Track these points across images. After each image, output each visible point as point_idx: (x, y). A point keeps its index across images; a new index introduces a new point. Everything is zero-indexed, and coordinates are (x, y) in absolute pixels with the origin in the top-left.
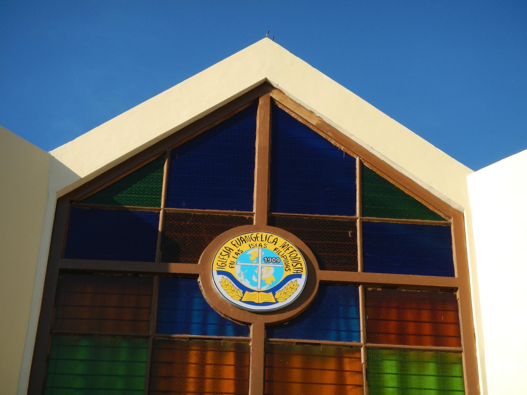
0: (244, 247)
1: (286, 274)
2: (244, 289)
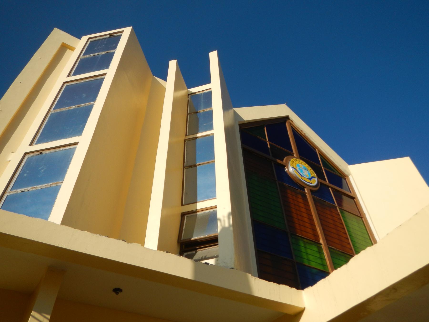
0: (297, 162)
2: (302, 176)
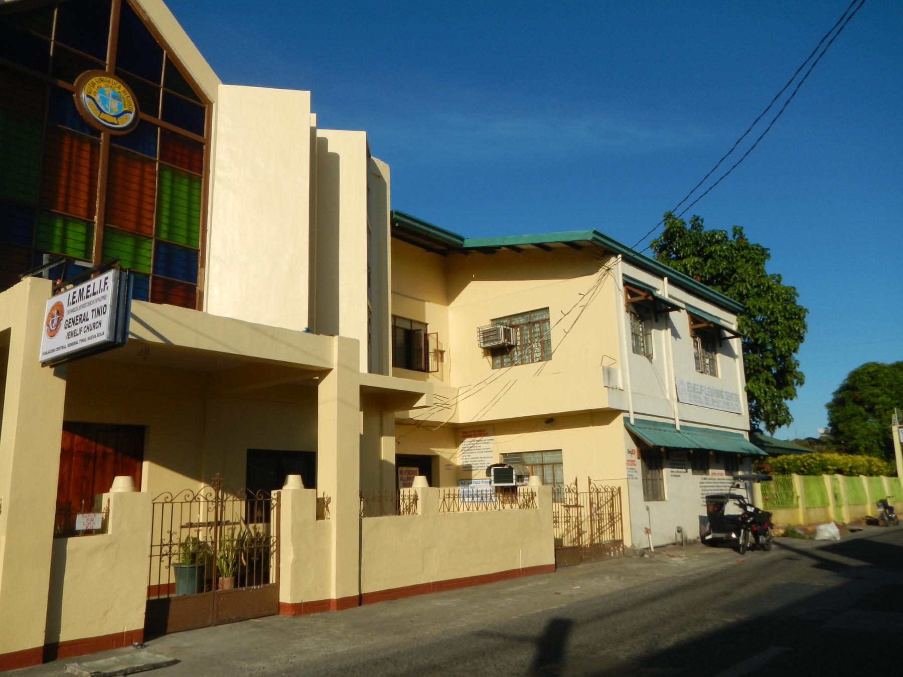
0: (103, 84)
1: (124, 109)
2: (102, 111)
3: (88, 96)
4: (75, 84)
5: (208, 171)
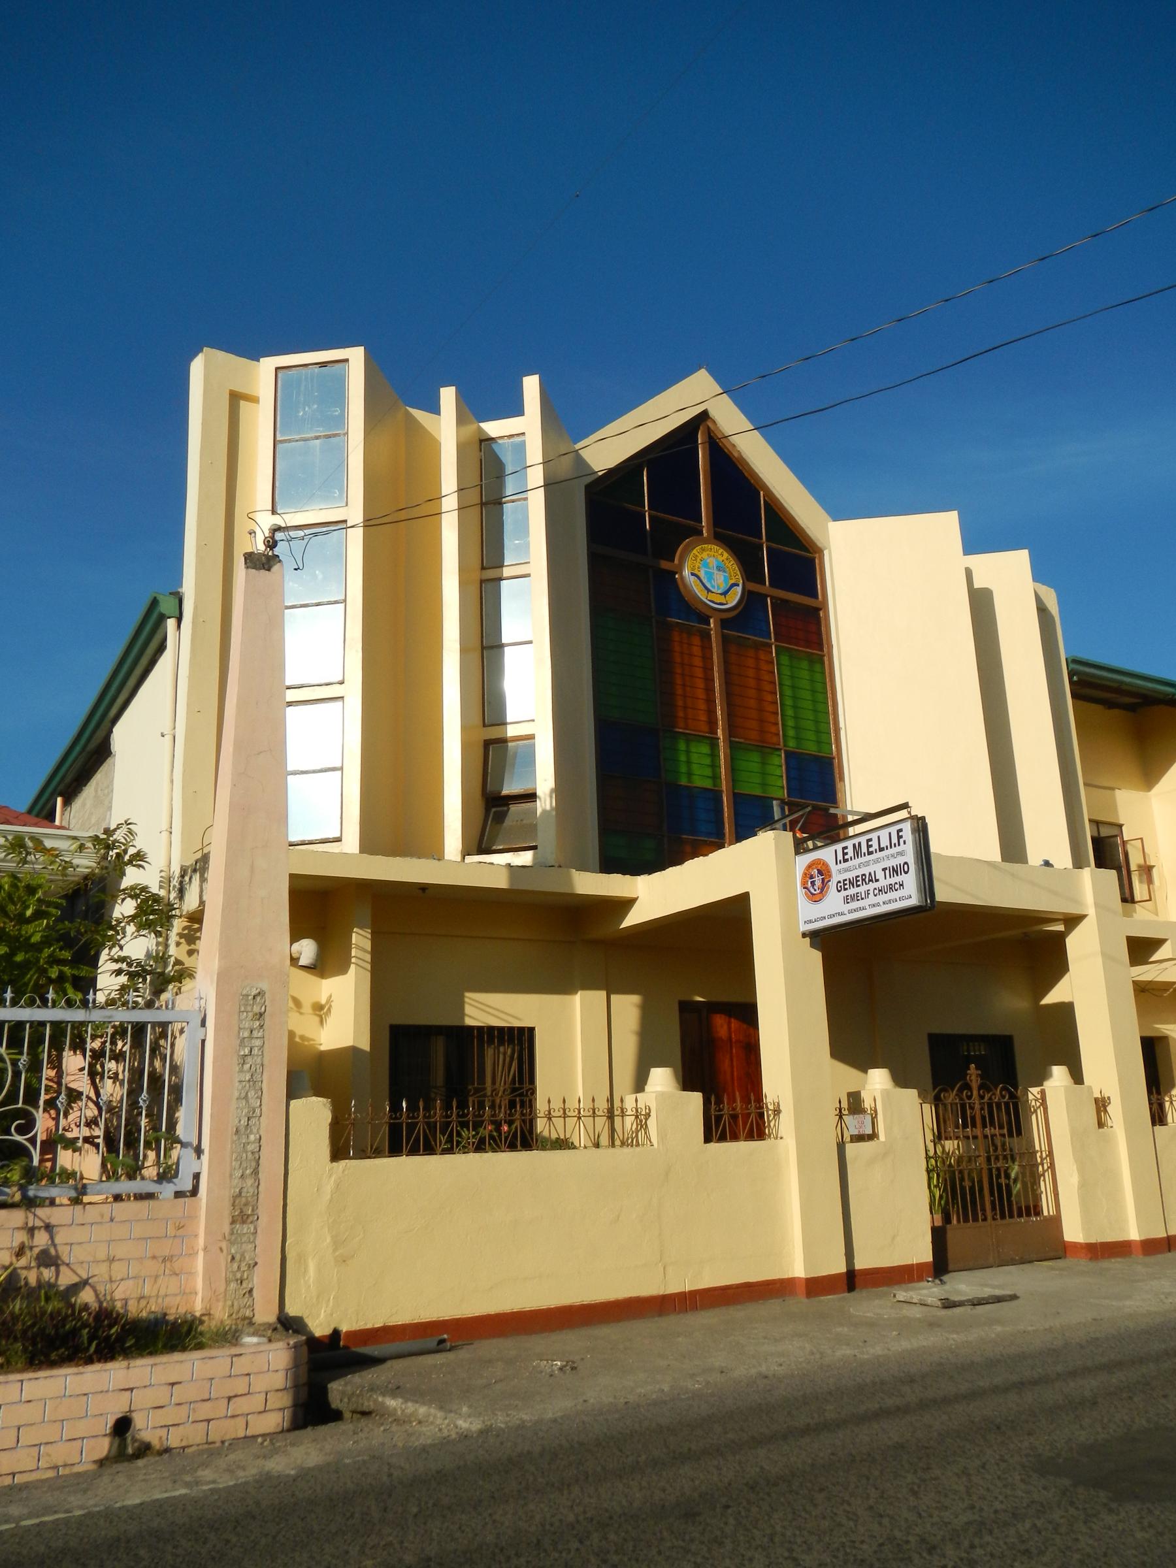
0: (705, 555)
2: (709, 590)
3: (693, 574)
4: (676, 561)
5: (830, 647)
